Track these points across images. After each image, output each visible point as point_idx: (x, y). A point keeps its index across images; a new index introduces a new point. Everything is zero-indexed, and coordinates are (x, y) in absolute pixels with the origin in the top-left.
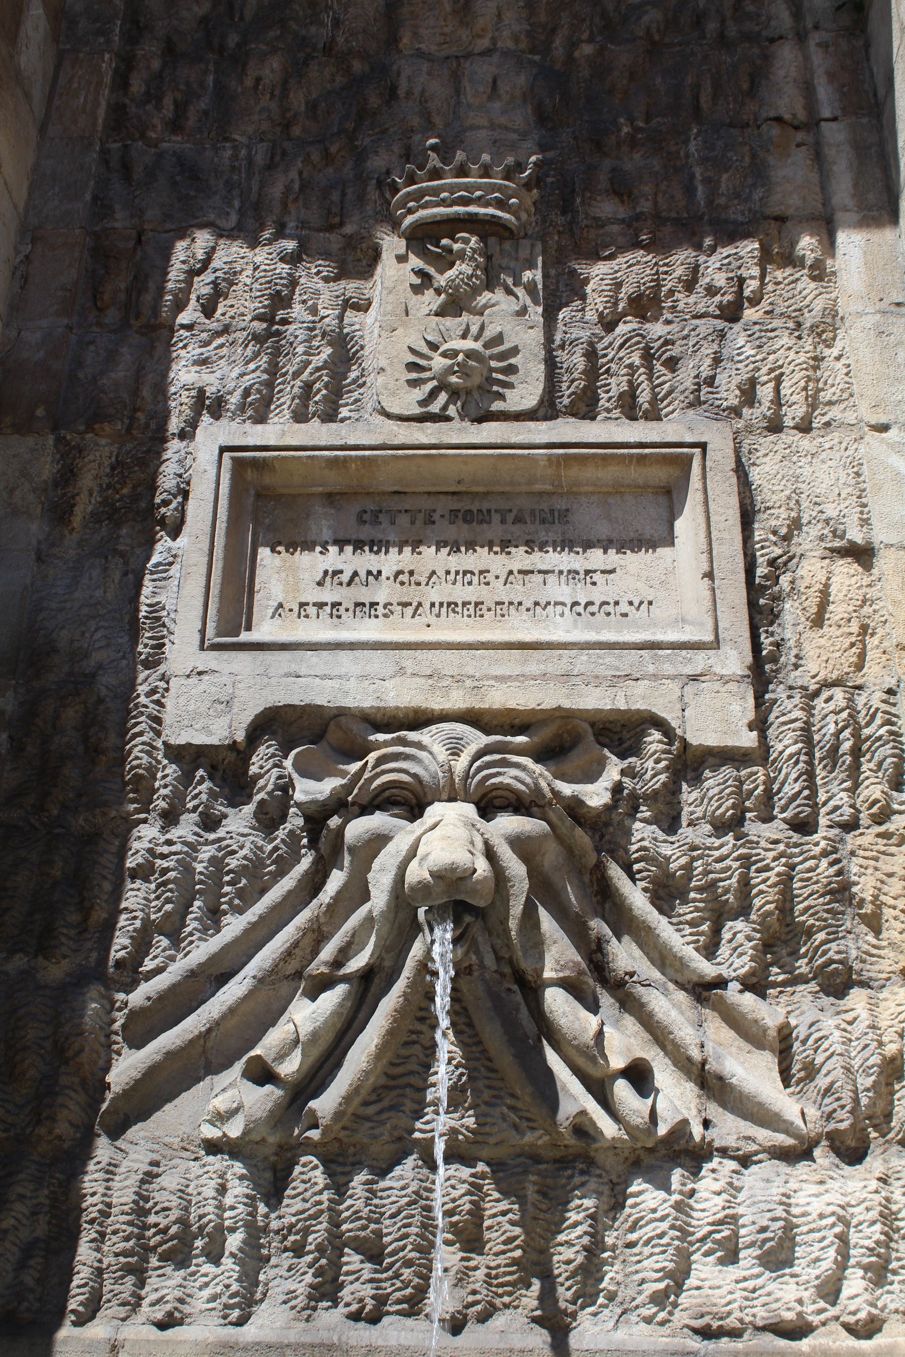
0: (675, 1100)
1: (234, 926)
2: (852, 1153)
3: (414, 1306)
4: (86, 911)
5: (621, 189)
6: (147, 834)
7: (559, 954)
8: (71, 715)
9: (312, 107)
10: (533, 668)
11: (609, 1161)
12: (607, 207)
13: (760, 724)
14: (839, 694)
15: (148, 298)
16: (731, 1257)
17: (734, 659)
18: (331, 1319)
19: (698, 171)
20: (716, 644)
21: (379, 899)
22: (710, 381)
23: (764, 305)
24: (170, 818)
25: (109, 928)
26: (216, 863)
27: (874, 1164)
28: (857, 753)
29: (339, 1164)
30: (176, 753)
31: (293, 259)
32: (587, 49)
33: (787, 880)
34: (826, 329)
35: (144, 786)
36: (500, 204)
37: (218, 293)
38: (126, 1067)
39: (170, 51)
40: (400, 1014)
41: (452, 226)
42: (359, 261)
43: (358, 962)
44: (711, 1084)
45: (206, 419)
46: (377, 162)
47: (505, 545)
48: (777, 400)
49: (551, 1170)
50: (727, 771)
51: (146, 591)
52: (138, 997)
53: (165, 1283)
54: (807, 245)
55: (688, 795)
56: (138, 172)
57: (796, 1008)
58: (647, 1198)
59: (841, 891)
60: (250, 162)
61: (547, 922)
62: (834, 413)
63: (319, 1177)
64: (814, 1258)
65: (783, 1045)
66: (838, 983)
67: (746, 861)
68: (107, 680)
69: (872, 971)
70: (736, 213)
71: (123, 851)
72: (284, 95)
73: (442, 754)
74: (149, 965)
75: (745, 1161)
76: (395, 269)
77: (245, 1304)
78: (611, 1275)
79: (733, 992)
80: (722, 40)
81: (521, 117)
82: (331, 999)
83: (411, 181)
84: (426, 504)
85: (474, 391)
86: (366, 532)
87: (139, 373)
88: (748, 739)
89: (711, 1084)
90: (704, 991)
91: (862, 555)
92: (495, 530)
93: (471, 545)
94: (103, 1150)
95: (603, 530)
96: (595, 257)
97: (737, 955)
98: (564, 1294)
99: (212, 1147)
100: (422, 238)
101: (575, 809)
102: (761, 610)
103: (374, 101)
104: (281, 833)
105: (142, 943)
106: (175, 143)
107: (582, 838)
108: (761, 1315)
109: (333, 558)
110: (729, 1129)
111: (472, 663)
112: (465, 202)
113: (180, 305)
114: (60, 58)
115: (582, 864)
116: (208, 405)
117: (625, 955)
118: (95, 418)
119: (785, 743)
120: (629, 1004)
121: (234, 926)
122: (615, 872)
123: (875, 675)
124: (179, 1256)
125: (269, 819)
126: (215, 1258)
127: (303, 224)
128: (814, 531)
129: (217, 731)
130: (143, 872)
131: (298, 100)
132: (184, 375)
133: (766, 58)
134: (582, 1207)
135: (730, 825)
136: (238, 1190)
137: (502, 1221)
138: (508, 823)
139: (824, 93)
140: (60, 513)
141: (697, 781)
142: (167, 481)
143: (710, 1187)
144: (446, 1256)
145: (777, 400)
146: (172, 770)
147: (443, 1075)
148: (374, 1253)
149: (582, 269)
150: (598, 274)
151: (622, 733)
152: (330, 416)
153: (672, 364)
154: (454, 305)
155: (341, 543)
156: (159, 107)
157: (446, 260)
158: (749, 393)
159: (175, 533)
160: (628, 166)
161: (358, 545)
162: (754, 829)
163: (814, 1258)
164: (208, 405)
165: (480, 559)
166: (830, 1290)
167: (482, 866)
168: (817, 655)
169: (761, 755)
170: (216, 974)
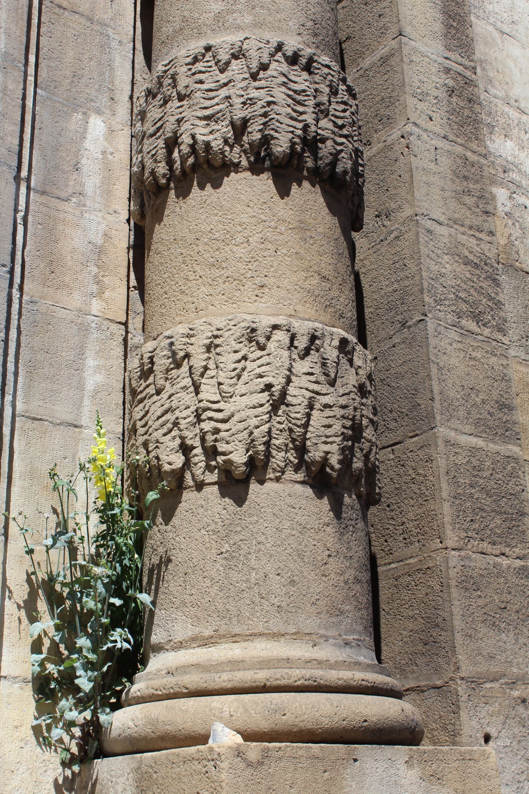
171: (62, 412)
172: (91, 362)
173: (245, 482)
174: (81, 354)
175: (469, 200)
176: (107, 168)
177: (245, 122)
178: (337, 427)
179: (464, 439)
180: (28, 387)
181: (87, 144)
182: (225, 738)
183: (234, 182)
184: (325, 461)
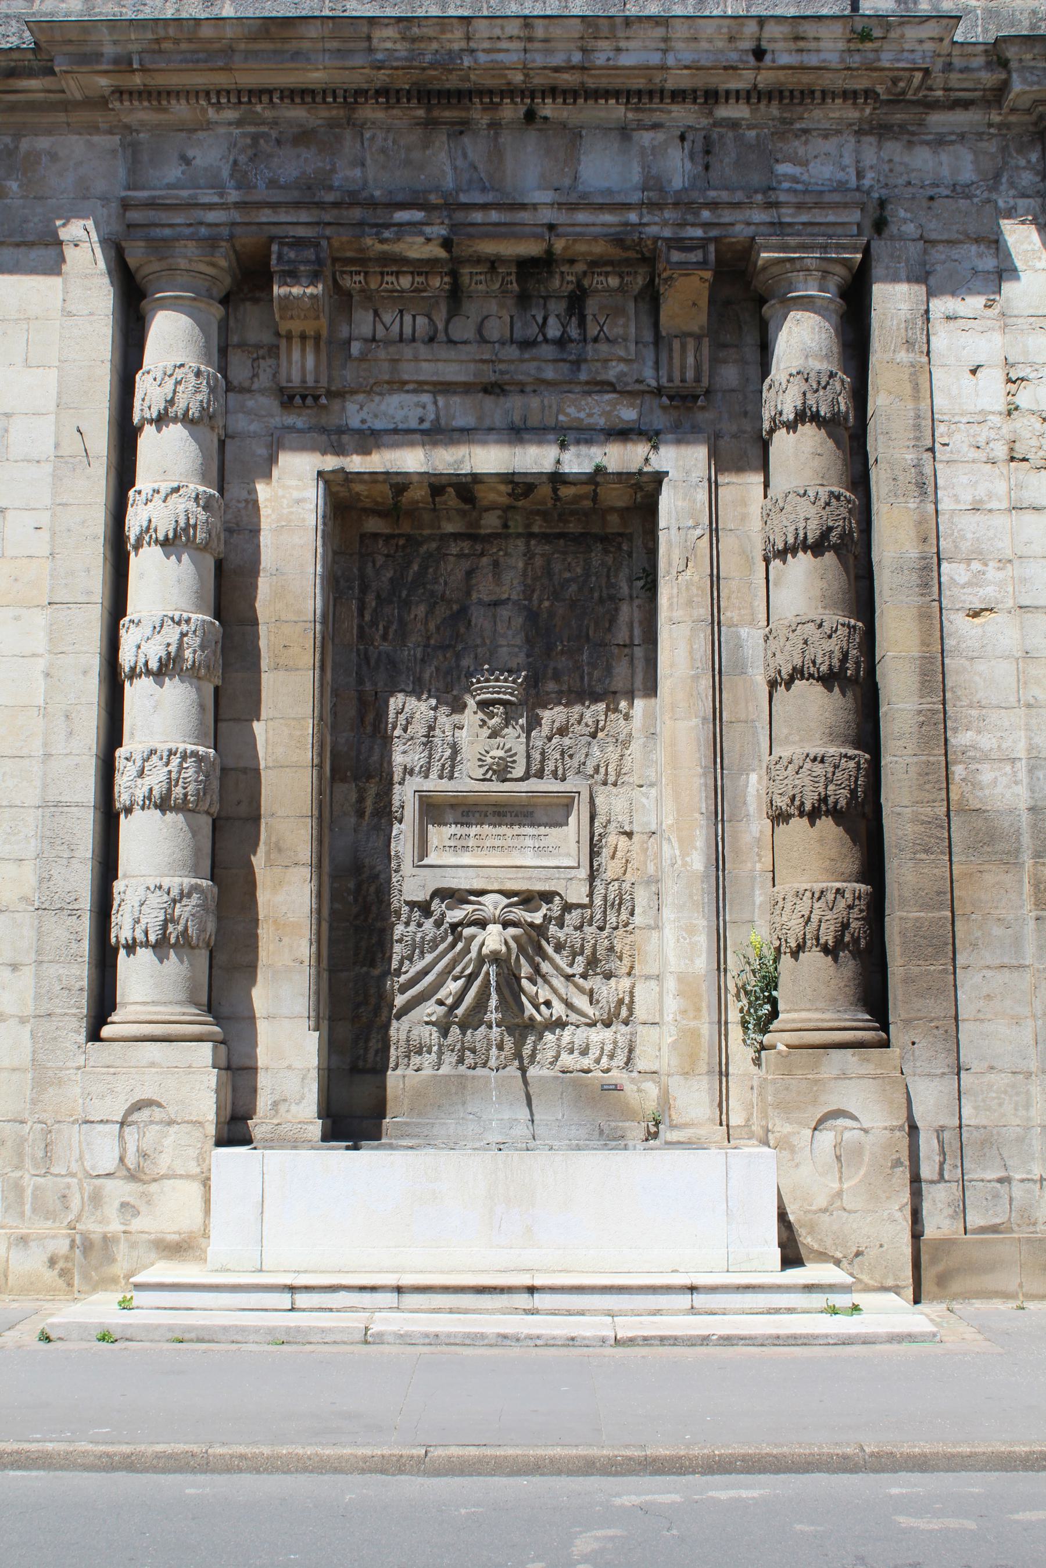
0: (558, 1009)
1: (429, 958)
2: (608, 1025)
3: (484, 1065)
4: (384, 953)
5: (557, 677)
6: (399, 930)
7: (526, 970)
8: (372, 889)
9: (438, 628)
10: (520, 875)
11: (539, 1027)
12: (551, 686)
13: (591, 895)
14: (616, 884)
15: (383, 726)
16: (572, 1052)
17: (584, 873)
18: (462, 1069)
19: (586, 669)
20: (578, 867)
21: (473, 954)
22: (584, 764)
23: (605, 732)
24: (407, 924)
25: (391, 957)
26: (422, 938)
27: (613, 1028)
28: (620, 904)
29: (463, 1027)
30: (407, 903)
31: (435, 709)
32: (546, 604)
33: (595, 945)
34: (626, 743)
35: (398, 913)
36: (511, 694)
37: (408, 722)
38: (400, 1000)
39: (378, 597)
40: (480, 987)
41: (493, 703)
42: (459, 707)
43: (468, 972)
44: (569, 1005)
45: (407, 777)
46: (466, 662)
47: (512, 825)
48: (606, 774)
49: (522, 1029)
50: (579, 911)
51: (393, 845)
52: (403, 979)
53: (416, 1060)
54: (623, 704)
55: (567, 917)
56: (373, 662)
57: (595, 982)
58: (549, 1037)
59: (611, 949)
60: (415, 655)
61: (522, 960)
62: (626, 778)
63: (458, 1031)
64: (594, 1053)
65: (591, 994)
66: (608, 976)
67: (583, 939)
68: (382, 876)
69: (619, 972)
70: (599, 689)
71: (392, 935)
72: (426, 624)
73: (491, 908)
74: (404, 969)
75: (578, 1026)
76: (471, 716)
77: (439, 1065)
78: (538, 1057)
79: (577, 979)
80: (601, 601)
81: (519, 640)
82: (461, 982)
83: (479, 682)
84: (485, 809)
85: (501, 771)
86: (464, 820)
87: (382, 757)
88: (586, 901)
89: (569, 1005)
90: (569, 977)
91: (629, 835)
92: (508, 819)
93: (500, 825)
94: (395, 1024)
95: (545, 820)
96: (544, 707)
97: (578, 968)
98: (526, 1062)
99: (427, 1023)
100: (483, 705)
101: (531, 925)
102: (594, 853)
103: (462, 630)
104: (442, 929)
105: (401, 963)
106: (385, 647)
107: (534, 934)
108: (579, 1067)
109: (453, 829)
110: (574, 1017)
111: (502, 873)
112: (498, 693)
113: (394, 728)
114: (335, 599)
115: (533, 942)
116: (409, 771)
117: (545, 967)
118: (369, 777)
119: (598, 901)
120: (546, 981)
121: (429, 958)
122: (544, 943)
123: (629, 877)
124: (419, 1053)
125: (438, 924)
126: (429, 1052)
127: (438, 690)
128: (614, 824)
129: (421, 896)
130: (400, 941)
131: (432, 626)
132: (398, 759)
133: (617, 610)
134: (531, 1039)
135: (579, 928)
136: (435, 1035)
137: (509, 1042)
138: (512, 931)
139: (637, 631)
140: (360, 814)
141: (570, 913)
142: (396, 803)
143: (567, 1034)
144: (494, 1051)
145: (606, 774)
146: (407, 908)
147: (493, 1002)
148: (473, 1051)
149: (539, 711)
150: (546, 715)
151: (547, 897)
152: (451, 777)
153: (571, 756)
154: (494, 735)
155: (456, 824)
156: (377, 630)
157: (492, 716)
158: (597, 770)
159: (400, 822)
160: (560, 666)
161: (462, 824)
162: (586, 928)
163: (594, 1053)
164: (409, 771)
165: (503, 830)
166: (598, 1061)
167: (504, 949)
168: (611, 869)
169: (591, 905)
170: (425, 972)
171: (746, 916)
172: (757, 892)
173: (798, 952)
174: (753, 889)
175: (927, 787)
176: (759, 796)
177: (794, 796)
178: (832, 928)
179: (911, 915)
180: (731, 909)
181: (750, 789)
182: (781, 1047)
183: (792, 821)
184: (826, 943)
